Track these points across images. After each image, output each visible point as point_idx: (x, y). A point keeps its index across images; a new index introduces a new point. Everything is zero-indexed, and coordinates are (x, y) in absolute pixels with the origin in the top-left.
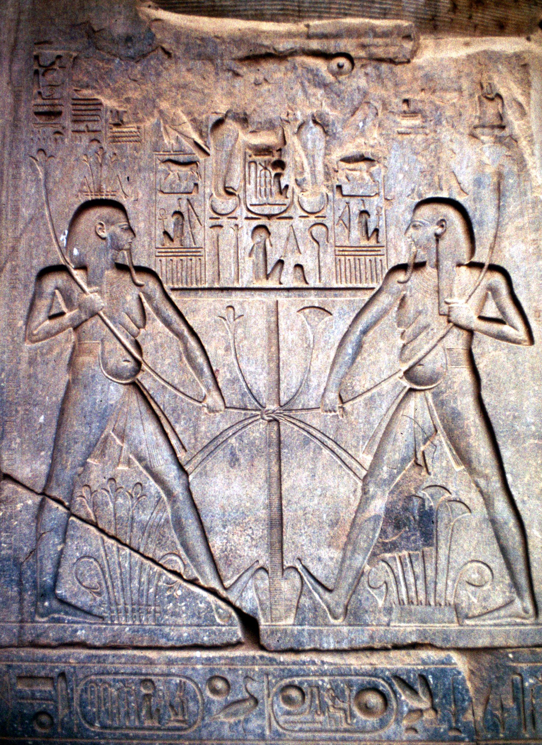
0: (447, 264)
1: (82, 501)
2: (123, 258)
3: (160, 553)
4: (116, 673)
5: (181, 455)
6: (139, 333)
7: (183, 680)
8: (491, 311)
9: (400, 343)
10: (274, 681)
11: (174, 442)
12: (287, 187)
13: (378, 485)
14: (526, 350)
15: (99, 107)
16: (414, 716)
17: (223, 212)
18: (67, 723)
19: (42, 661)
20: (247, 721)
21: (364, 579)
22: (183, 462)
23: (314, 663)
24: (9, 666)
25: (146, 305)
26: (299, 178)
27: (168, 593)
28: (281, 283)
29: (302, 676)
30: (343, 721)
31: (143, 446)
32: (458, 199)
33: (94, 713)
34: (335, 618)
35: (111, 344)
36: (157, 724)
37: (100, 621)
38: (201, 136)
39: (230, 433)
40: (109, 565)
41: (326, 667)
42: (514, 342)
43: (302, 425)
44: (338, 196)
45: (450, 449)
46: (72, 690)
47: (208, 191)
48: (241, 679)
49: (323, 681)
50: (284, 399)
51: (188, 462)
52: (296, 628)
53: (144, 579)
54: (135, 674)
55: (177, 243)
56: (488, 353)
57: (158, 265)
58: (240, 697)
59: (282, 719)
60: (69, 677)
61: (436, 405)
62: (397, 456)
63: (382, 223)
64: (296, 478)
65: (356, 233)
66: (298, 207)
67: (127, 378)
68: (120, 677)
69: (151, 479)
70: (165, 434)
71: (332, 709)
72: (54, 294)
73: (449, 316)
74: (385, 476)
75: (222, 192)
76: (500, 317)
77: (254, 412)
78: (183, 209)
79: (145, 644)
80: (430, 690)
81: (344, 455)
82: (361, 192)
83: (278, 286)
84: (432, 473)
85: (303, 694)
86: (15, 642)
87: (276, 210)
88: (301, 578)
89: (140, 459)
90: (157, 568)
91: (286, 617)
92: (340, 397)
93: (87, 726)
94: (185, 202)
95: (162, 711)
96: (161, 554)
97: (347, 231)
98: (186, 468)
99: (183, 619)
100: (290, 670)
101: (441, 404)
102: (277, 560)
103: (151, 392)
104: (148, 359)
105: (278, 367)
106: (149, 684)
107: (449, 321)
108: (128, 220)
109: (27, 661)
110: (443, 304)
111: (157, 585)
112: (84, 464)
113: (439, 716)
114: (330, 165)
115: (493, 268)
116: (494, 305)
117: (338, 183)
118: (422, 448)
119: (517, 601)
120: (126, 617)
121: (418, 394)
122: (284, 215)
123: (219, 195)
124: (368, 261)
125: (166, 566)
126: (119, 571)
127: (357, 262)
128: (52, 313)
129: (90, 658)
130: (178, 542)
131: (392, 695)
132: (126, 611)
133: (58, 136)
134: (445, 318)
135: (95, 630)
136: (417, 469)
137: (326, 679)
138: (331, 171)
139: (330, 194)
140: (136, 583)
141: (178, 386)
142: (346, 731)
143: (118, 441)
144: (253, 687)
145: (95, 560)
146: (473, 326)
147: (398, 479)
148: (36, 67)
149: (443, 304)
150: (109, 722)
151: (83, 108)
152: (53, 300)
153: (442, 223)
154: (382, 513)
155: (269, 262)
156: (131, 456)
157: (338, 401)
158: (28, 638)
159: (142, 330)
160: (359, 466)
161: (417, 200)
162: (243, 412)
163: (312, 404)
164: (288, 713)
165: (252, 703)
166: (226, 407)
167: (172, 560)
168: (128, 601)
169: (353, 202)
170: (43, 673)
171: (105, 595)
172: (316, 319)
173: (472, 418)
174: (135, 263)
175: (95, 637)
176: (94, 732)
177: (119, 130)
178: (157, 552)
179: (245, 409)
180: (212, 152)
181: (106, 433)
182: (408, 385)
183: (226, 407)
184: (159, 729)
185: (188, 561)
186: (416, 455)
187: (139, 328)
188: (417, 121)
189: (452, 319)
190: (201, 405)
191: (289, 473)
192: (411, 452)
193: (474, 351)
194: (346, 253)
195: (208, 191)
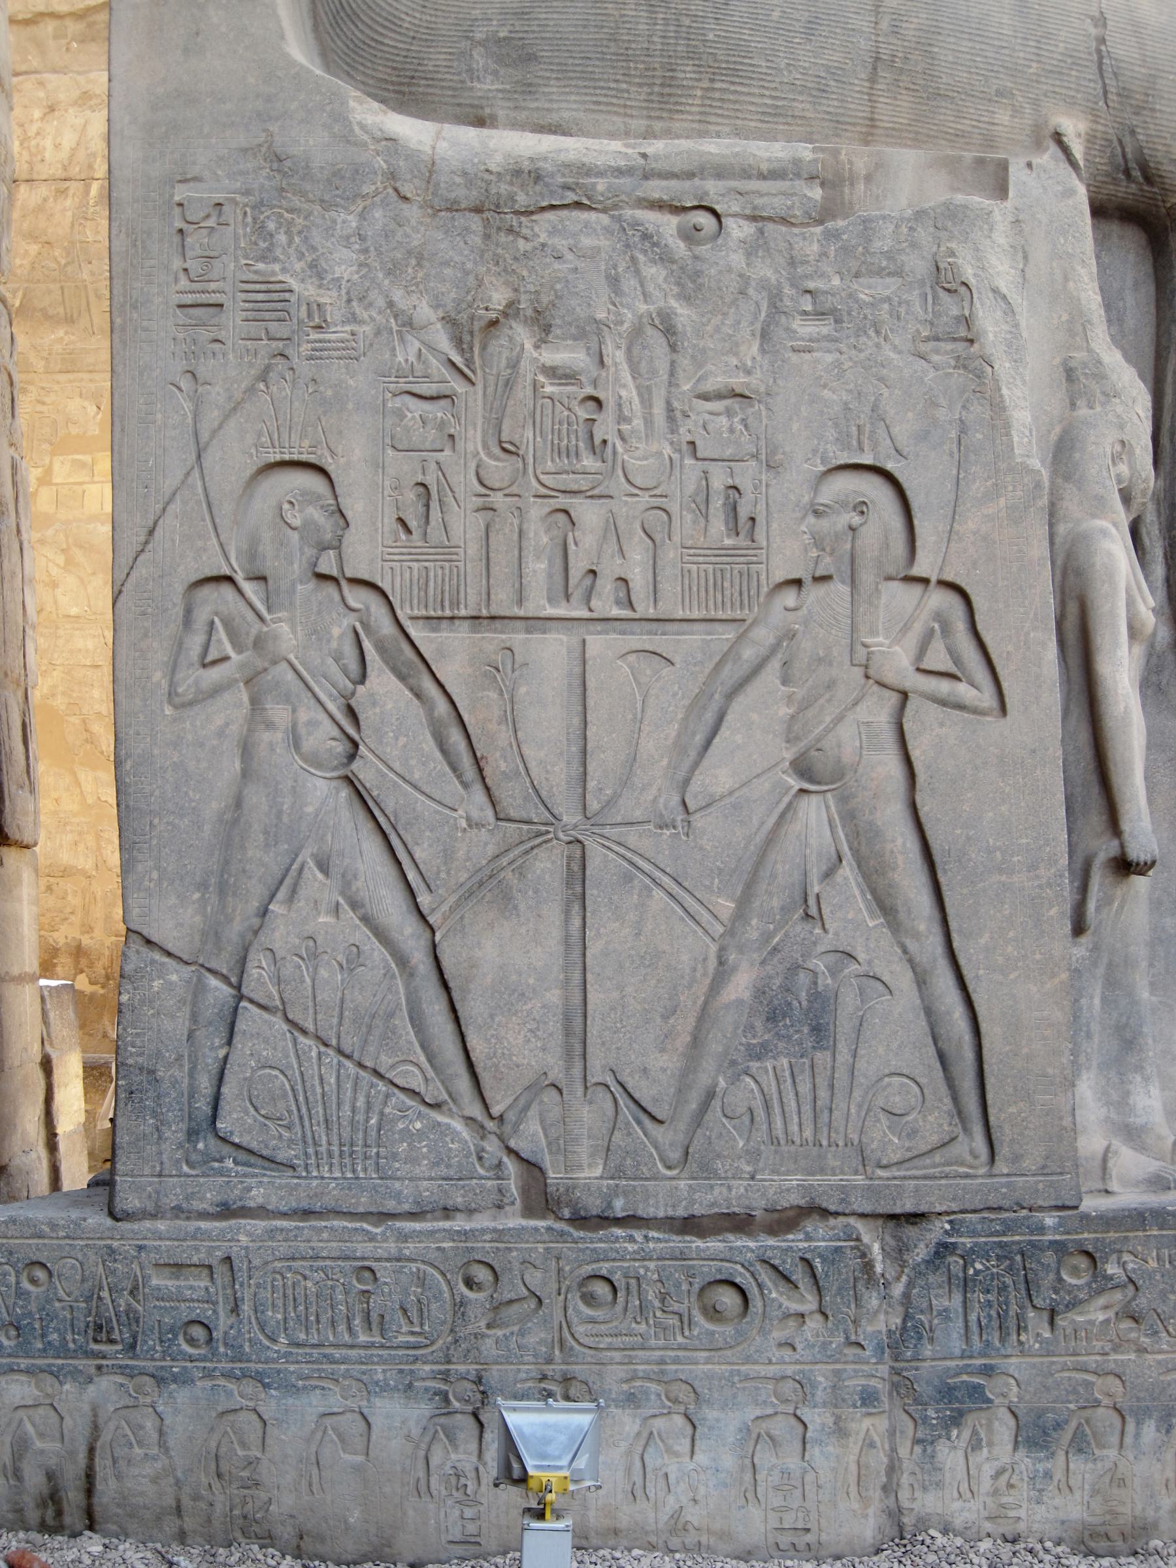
0: (867, 577)
1: (261, 975)
2: (328, 565)
3: (385, 1062)
4: (316, 1258)
5: (424, 899)
6: (353, 693)
7: (423, 1267)
8: (938, 659)
9: (785, 711)
10: (567, 1268)
11: (411, 875)
12: (605, 442)
13: (741, 950)
14: (994, 726)
15: (287, 296)
16: (791, 1323)
17: (497, 485)
18: (235, 1338)
19: (194, 1238)
20: (522, 1333)
21: (716, 1104)
22: (425, 911)
23: (632, 1239)
24: (140, 1248)
25: (367, 645)
26: (625, 427)
27: (401, 1126)
28: (590, 610)
29: (614, 1260)
30: (677, 1331)
31: (359, 884)
32: (889, 466)
33: (278, 1322)
34: (669, 1168)
35: (307, 713)
36: (378, 1339)
37: (290, 1173)
38: (462, 351)
39: (504, 861)
40: (303, 1081)
41: (651, 1245)
42: (975, 711)
43: (622, 850)
44: (689, 461)
45: (863, 893)
46: (242, 1285)
47: (470, 447)
48: (516, 1265)
49: (647, 1269)
50: (594, 805)
51: (433, 910)
52: (605, 1182)
53: (361, 1103)
54: (347, 1258)
55: (416, 535)
56: (931, 733)
57: (388, 578)
58: (513, 1296)
59: (580, 1329)
60: (236, 1262)
61: (841, 818)
62: (776, 903)
63: (761, 506)
64: (609, 935)
65: (718, 524)
66: (623, 480)
67: (335, 769)
68: (321, 1263)
69: (374, 939)
70: (399, 863)
71: (659, 1314)
72: (212, 623)
73: (866, 667)
74: (754, 935)
75: (497, 451)
76: (953, 669)
77: (543, 828)
78: (430, 480)
79: (361, 1210)
80: (816, 1283)
81: (689, 901)
82: (728, 453)
83: (585, 614)
84: (831, 931)
85: (615, 1290)
86: (150, 1206)
87: (583, 483)
88: (615, 1100)
89: (354, 905)
90: (382, 1086)
91: (590, 1165)
92: (684, 803)
93: (266, 1342)
94: (433, 466)
95: (387, 1318)
96: (390, 1061)
97: (702, 520)
98: (431, 920)
99: (423, 1169)
100: (595, 1250)
101: (849, 817)
102: (577, 1071)
103: (375, 793)
104: (368, 737)
105: (584, 752)
106: (367, 1274)
107: (867, 677)
108: (336, 498)
109: (169, 1239)
110: (859, 647)
111: (382, 1114)
112: (264, 912)
113: (830, 1324)
114: (676, 404)
115: (945, 584)
116: (942, 648)
117: (689, 438)
118: (816, 889)
119: (961, 1137)
120: (331, 1165)
121: (814, 799)
122: (596, 492)
123: (490, 455)
124: (735, 572)
125: (396, 1081)
126: (319, 1090)
127: (719, 575)
128: (209, 658)
129: (271, 1233)
130: (416, 1044)
131: (756, 1290)
132: (330, 1154)
133: (217, 346)
134: (862, 669)
135: (280, 1187)
136: (808, 926)
137: (652, 1265)
138: (678, 414)
139: (676, 456)
140: (346, 1111)
141: (420, 784)
142: (681, 1348)
143: (320, 876)
144: (535, 1278)
145: (282, 1072)
146: (907, 685)
147: (777, 939)
148: (179, 224)
149: (859, 647)
150: (303, 1336)
151: (260, 297)
152: (210, 634)
153: (861, 508)
154: (747, 995)
155: (572, 572)
156: (341, 901)
157: (681, 808)
158: (171, 1201)
159: (361, 689)
160: (711, 919)
161: (822, 468)
162: (525, 827)
163: (638, 814)
164: (593, 1321)
165: (533, 1304)
166: (498, 819)
167: (407, 1072)
168: (335, 1141)
169: (713, 468)
170: (195, 1260)
171: (298, 1129)
172: (648, 672)
173: (899, 841)
174: (349, 574)
175: (281, 1199)
176: (277, 1352)
177: (321, 336)
178: (383, 1058)
179: (529, 822)
180: (478, 379)
181: (299, 859)
182: (795, 783)
183: (498, 819)
184: (382, 1346)
185: (431, 1073)
186: (806, 901)
187: (355, 683)
188: (825, 328)
189: (871, 672)
190: (454, 815)
191: (598, 930)
192: (798, 898)
193: (906, 727)
194: (701, 559)
195: (470, 447)
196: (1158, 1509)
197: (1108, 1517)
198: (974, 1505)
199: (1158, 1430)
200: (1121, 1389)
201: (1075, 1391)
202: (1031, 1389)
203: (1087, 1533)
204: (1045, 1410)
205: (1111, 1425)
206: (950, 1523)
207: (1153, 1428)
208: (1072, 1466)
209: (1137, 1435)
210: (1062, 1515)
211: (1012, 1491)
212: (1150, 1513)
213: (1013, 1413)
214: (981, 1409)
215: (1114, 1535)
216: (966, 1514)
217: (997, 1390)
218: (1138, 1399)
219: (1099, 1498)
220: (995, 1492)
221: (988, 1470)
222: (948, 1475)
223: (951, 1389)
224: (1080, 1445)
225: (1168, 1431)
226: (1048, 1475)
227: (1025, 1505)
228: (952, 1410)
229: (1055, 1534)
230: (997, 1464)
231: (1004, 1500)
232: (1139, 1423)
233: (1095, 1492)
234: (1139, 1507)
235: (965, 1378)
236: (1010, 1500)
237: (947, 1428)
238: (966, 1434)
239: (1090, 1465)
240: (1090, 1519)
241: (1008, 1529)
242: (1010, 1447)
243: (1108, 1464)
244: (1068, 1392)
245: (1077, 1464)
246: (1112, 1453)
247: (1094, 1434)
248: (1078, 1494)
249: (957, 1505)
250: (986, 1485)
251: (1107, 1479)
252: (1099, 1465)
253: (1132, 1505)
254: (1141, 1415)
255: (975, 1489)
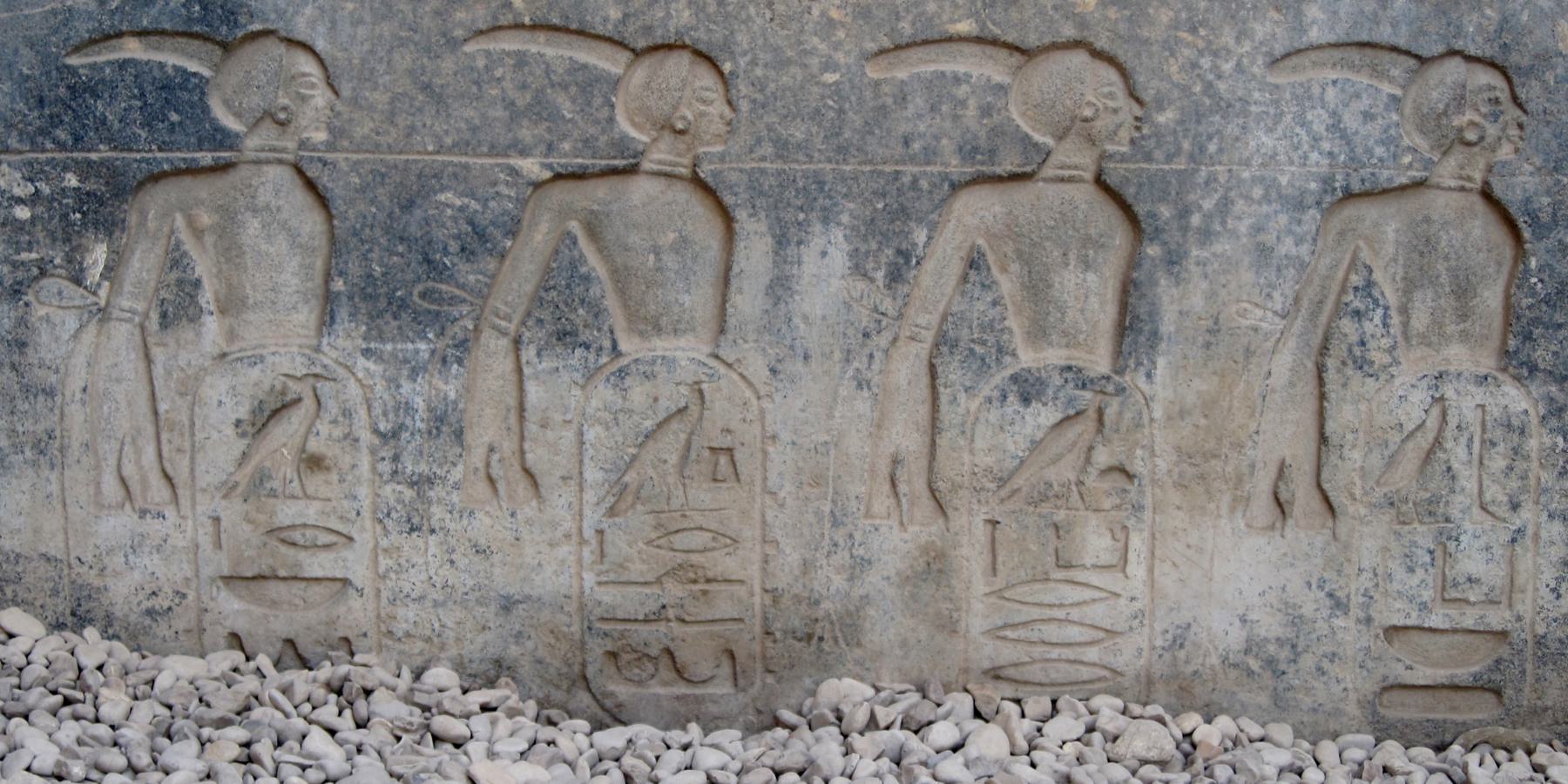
196: (859, 566)
197: (674, 591)
198: (183, 529)
199: (858, 269)
200: (719, 108)
201: (540, 110)
202: (380, 98)
203: (597, 648)
204: (429, 180)
205: (683, 243)
206: (92, 593)
207: (839, 259)
208: (534, 391)
209: (780, 287)
210: (503, 579)
211: (315, 482)
212: (831, 580)
213: (311, 185)
214: (193, 170)
215: (698, 655)
216: (149, 561)
217: (255, 101)
218: (783, 149)
219: (639, 519)
220: (259, 486)
221: (225, 400)
222: (77, 415)
223: (83, 89)
224: (563, 318)
225: (895, 277)
226: (447, 425)
227: (365, 534)
228: (86, 170)
229: (478, 646)
230: (255, 380)
231: (287, 513)
232: (784, 240)
233: (620, 497)
234: (791, 556)
235: (133, 49)
236: (311, 512)
237: (69, 239)
238: (144, 264)
239: (603, 394)
240: (608, 596)
241: (297, 616)
242: (306, 316)
243: (672, 395)
244: (515, 115)
245: (554, 385)
246: (688, 350)
247: (621, 277)
248: (560, 500)
249: (116, 526)
250: (221, 449)
251: (669, 447)
252: (638, 393)
253: (767, 549)
254: (795, 208)
255: (181, 472)
